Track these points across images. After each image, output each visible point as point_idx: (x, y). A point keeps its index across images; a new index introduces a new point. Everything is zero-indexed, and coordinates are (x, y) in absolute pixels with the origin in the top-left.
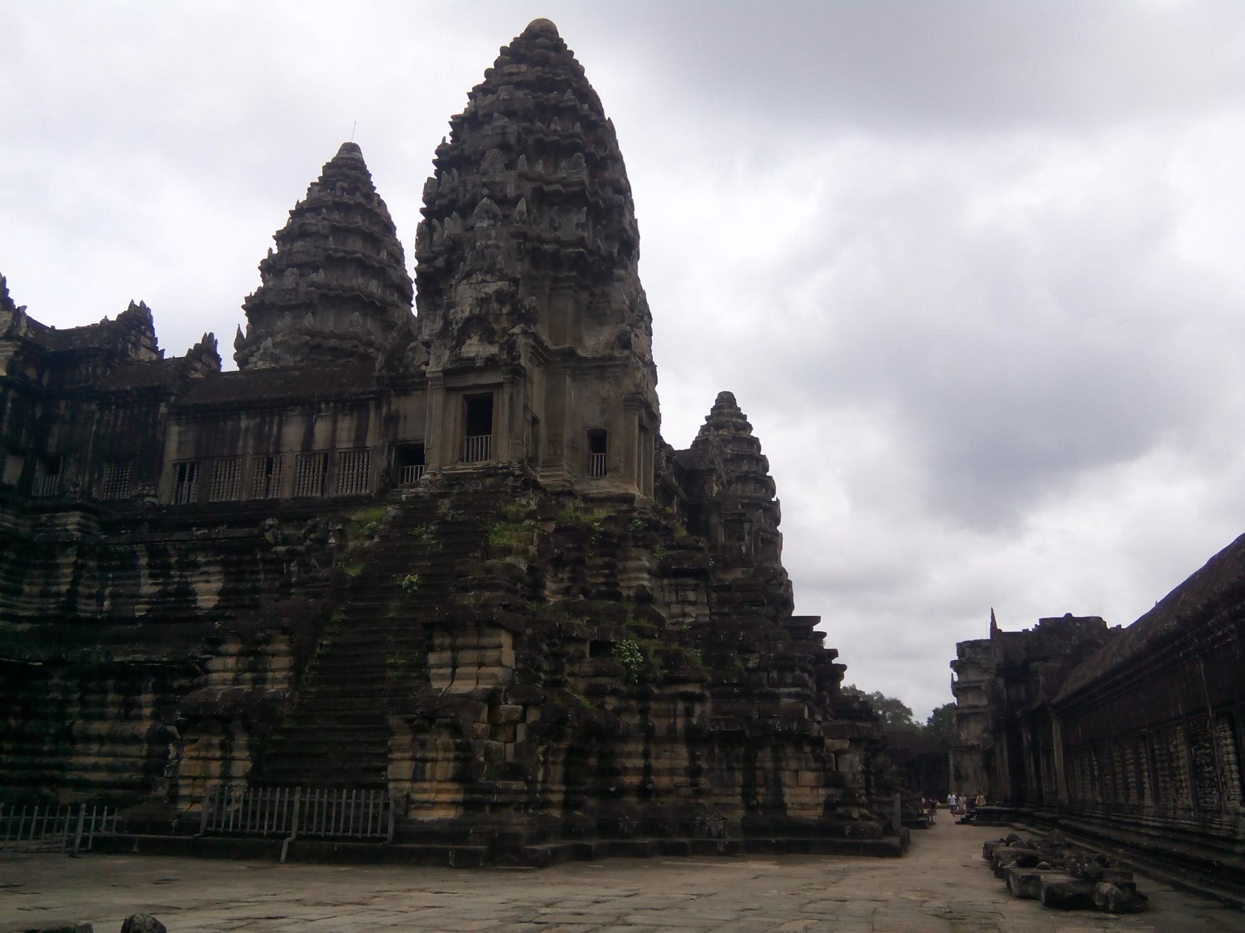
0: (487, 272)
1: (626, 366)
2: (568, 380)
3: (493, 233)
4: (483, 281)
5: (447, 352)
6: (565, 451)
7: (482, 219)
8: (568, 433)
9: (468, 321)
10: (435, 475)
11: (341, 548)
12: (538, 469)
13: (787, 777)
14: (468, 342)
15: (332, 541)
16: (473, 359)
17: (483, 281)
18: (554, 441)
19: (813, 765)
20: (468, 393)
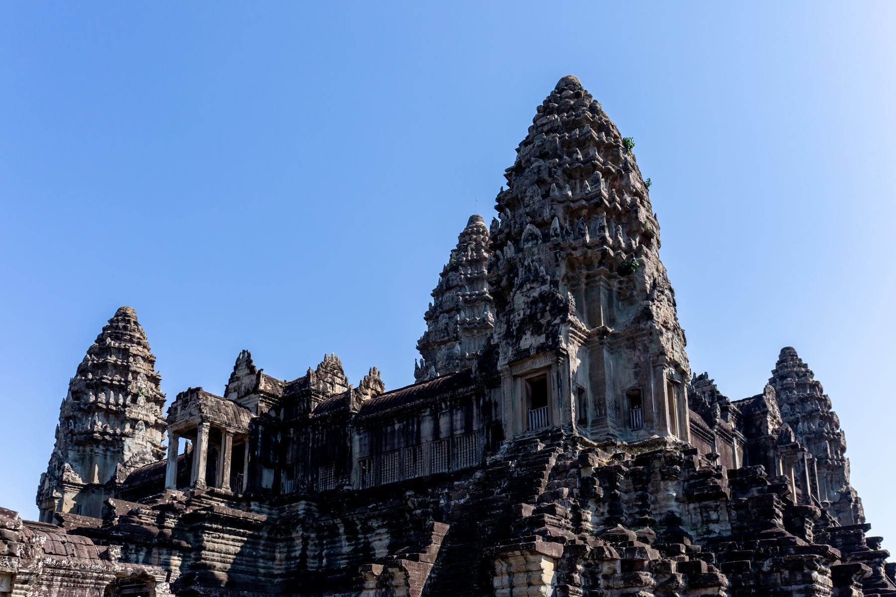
0: (533, 281)
1: (651, 334)
2: (606, 354)
3: (535, 250)
4: (531, 288)
5: (511, 349)
6: (609, 412)
7: (527, 240)
8: (609, 396)
9: (522, 321)
10: (510, 443)
11: (448, 505)
12: (589, 428)
14: (524, 337)
15: (442, 501)
16: (528, 350)
17: (531, 288)
18: (599, 404)
20: (529, 377)
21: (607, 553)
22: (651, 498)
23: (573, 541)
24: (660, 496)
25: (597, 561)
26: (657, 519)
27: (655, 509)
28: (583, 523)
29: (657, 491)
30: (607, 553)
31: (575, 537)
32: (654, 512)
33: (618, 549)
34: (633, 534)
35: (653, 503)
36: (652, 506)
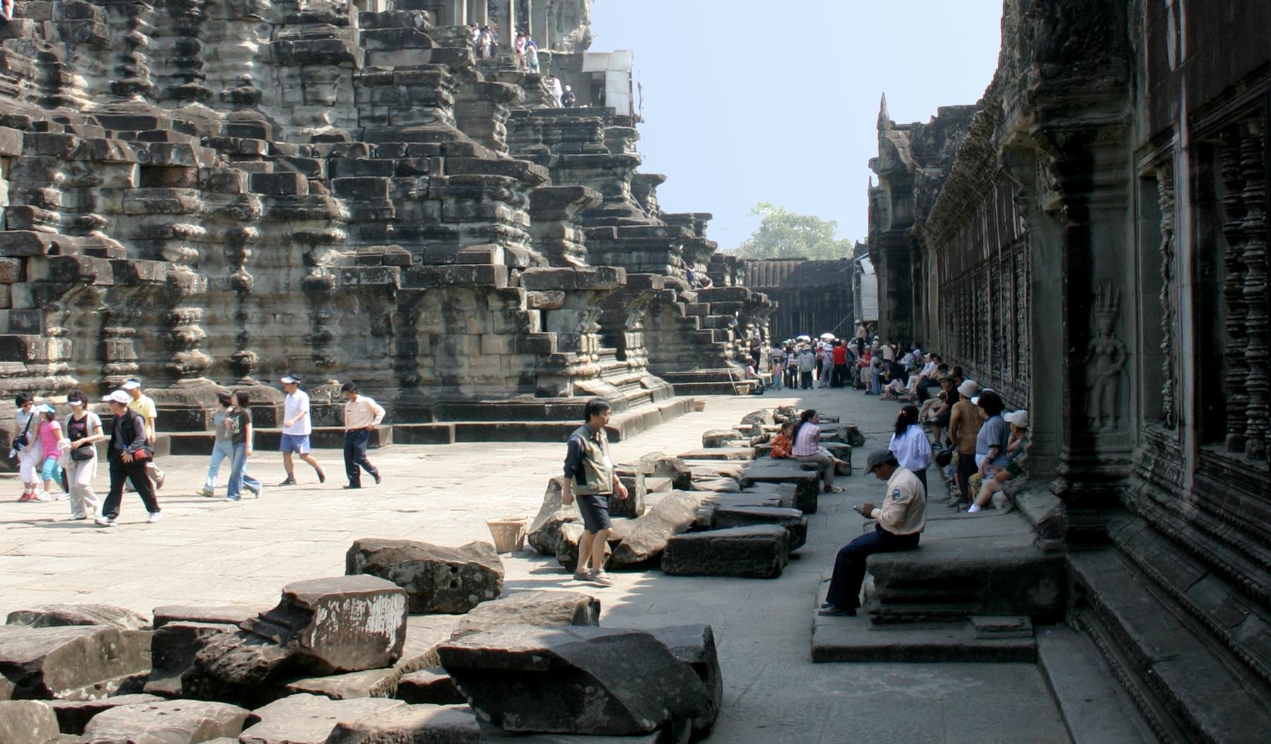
13: (465, 344)
19: (501, 325)
21: (114, 151)
22: (206, 49)
23: (42, 126)
24: (224, 47)
25: (91, 165)
26: (215, 91)
27: (211, 71)
28: (63, 88)
29: (219, 38)
30: (114, 151)
31: (46, 115)
32: (209, 77)
33: (136, 146)
34: (165, 114)
35: (209, 58)
36: (206, 65)
